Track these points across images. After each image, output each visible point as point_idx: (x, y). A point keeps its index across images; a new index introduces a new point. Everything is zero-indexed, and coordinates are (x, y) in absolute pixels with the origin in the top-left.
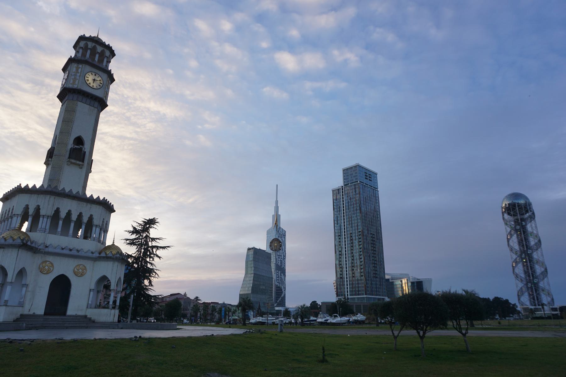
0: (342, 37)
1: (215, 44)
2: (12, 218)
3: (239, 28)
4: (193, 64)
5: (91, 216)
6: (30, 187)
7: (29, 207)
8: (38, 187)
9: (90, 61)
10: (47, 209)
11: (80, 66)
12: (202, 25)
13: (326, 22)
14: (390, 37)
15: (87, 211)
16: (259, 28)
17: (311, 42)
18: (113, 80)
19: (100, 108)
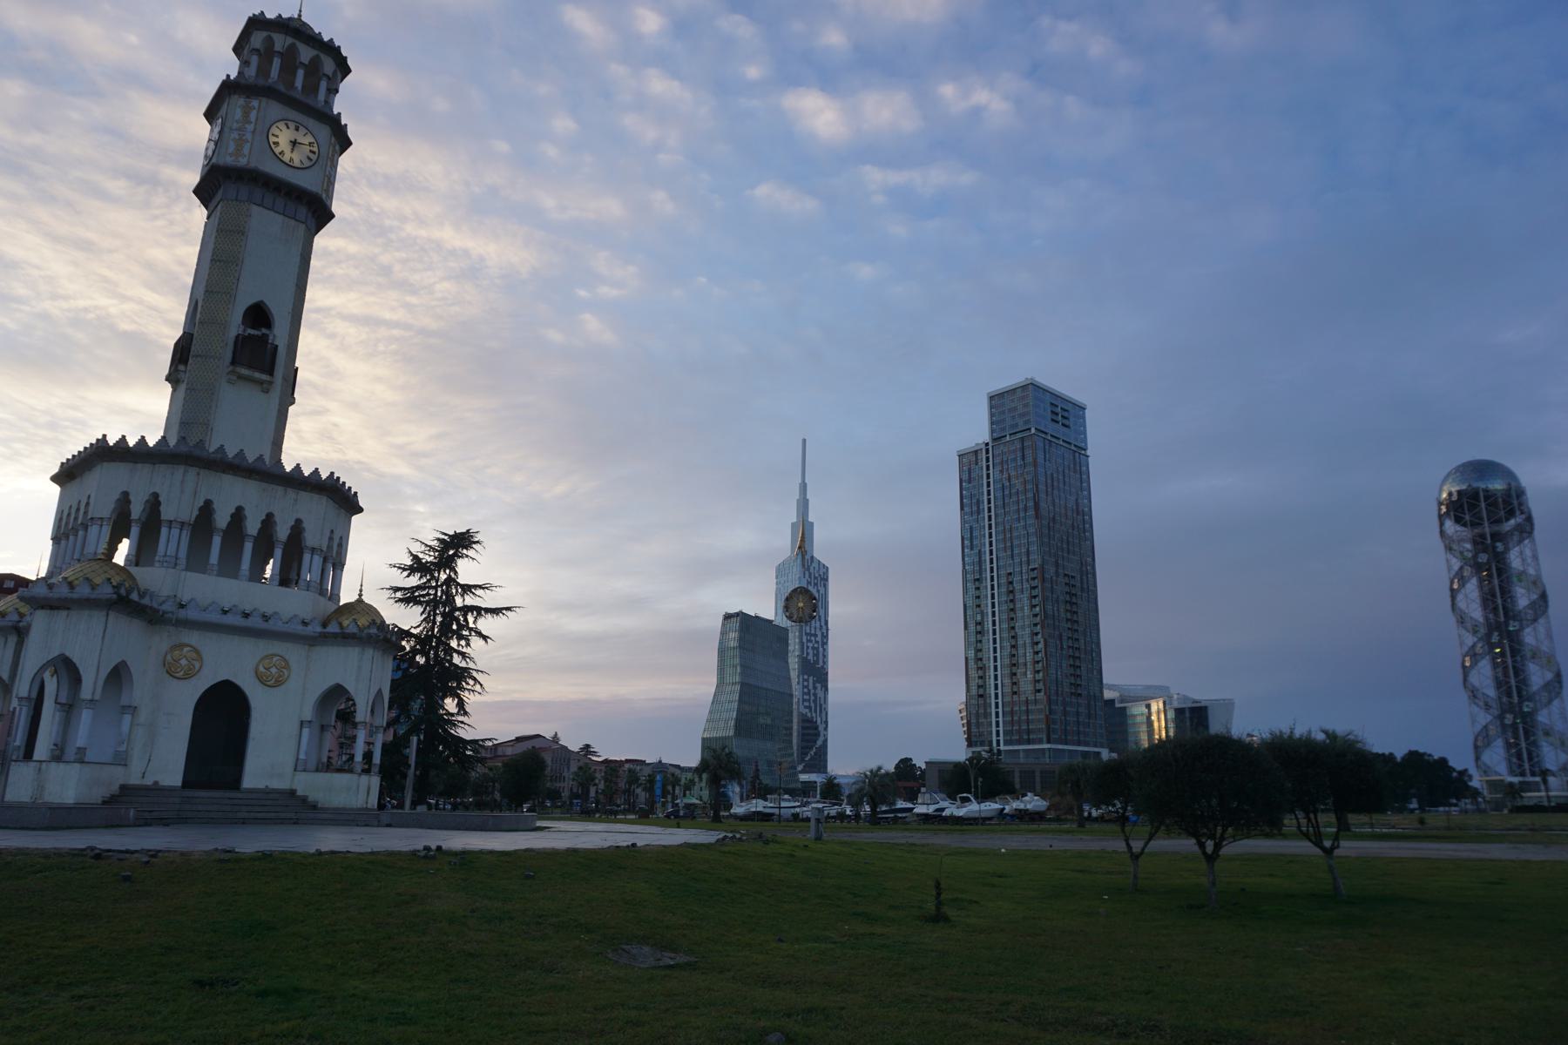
0: (964, 47)
1: (618, 70)
2: (86, 527)
3: (683, 26)
4: (563, 124)
5: (299, 522)
6: (132, 442)
7: (132, 498)
8: (151, 442)
9: (281, 88)
10: (179, 503)
11: (255, 103)
14: (1098, 47)
15: (288, 509)
16: (741, 28)
17: (883, 60)
18: (345, 143)
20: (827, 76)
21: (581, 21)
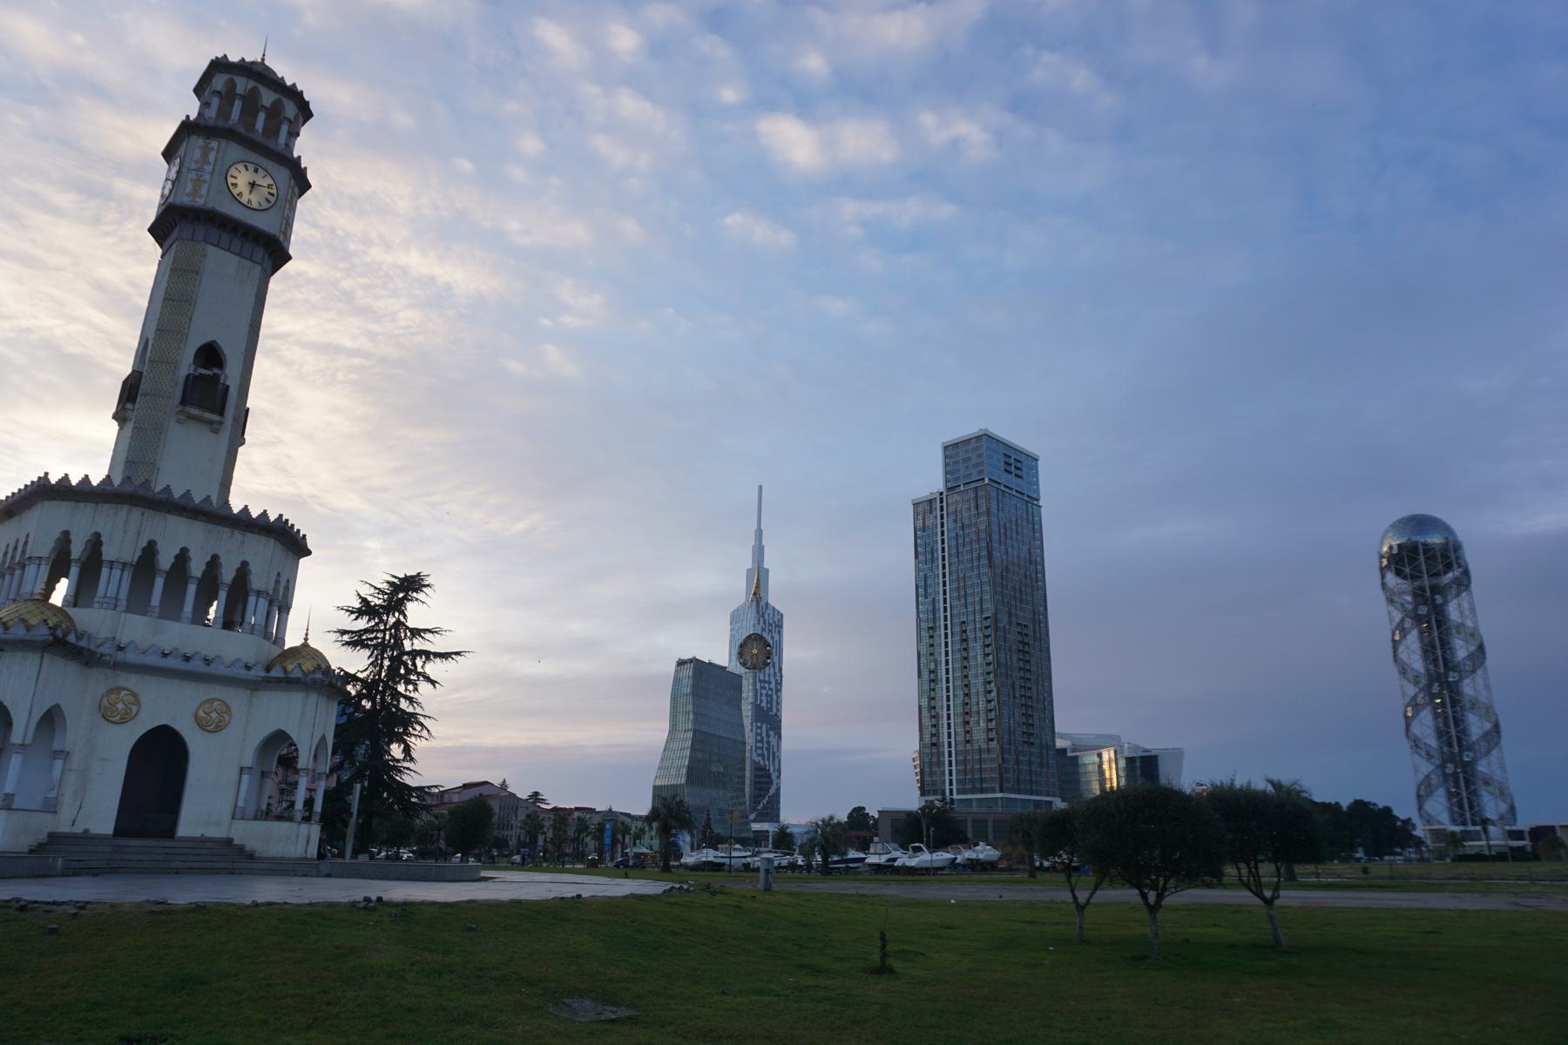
0: (947, 76)
1: (591, 90)
2: (23, 567)
3: (659, 47)
4: (531, 144)
5: (245, 564)
6: (74, 481)
7: (72, 537)
8: (95, 483)
9: (242, 130)
11: (214, 144)
12: (554, 36)
13: (901, 33)
14: (1081, 79)
15: (232, 551)
16: (714, 48)
17: (860, 89)
18: (303, 185)
19: (269, 265)
20: (804, 103)
21: (554, 36)
